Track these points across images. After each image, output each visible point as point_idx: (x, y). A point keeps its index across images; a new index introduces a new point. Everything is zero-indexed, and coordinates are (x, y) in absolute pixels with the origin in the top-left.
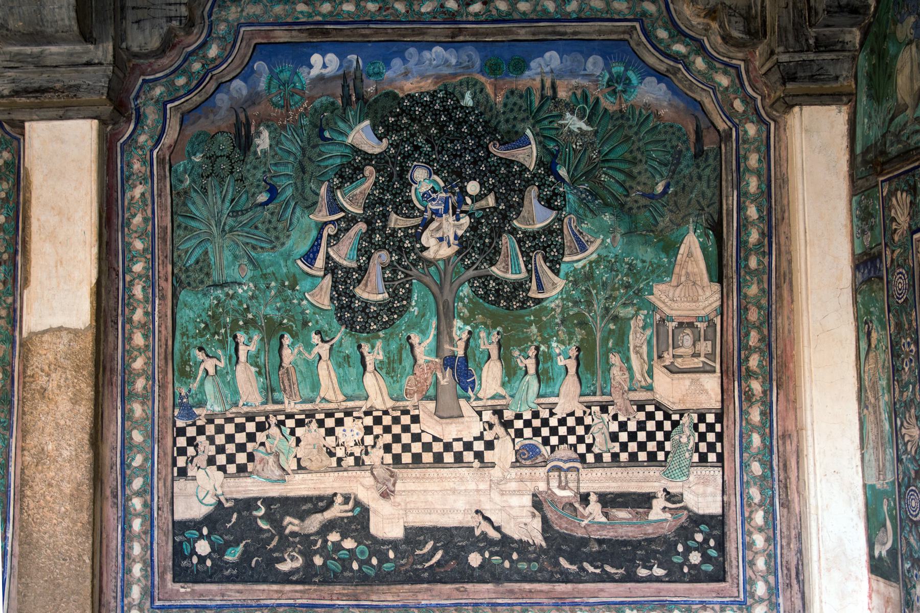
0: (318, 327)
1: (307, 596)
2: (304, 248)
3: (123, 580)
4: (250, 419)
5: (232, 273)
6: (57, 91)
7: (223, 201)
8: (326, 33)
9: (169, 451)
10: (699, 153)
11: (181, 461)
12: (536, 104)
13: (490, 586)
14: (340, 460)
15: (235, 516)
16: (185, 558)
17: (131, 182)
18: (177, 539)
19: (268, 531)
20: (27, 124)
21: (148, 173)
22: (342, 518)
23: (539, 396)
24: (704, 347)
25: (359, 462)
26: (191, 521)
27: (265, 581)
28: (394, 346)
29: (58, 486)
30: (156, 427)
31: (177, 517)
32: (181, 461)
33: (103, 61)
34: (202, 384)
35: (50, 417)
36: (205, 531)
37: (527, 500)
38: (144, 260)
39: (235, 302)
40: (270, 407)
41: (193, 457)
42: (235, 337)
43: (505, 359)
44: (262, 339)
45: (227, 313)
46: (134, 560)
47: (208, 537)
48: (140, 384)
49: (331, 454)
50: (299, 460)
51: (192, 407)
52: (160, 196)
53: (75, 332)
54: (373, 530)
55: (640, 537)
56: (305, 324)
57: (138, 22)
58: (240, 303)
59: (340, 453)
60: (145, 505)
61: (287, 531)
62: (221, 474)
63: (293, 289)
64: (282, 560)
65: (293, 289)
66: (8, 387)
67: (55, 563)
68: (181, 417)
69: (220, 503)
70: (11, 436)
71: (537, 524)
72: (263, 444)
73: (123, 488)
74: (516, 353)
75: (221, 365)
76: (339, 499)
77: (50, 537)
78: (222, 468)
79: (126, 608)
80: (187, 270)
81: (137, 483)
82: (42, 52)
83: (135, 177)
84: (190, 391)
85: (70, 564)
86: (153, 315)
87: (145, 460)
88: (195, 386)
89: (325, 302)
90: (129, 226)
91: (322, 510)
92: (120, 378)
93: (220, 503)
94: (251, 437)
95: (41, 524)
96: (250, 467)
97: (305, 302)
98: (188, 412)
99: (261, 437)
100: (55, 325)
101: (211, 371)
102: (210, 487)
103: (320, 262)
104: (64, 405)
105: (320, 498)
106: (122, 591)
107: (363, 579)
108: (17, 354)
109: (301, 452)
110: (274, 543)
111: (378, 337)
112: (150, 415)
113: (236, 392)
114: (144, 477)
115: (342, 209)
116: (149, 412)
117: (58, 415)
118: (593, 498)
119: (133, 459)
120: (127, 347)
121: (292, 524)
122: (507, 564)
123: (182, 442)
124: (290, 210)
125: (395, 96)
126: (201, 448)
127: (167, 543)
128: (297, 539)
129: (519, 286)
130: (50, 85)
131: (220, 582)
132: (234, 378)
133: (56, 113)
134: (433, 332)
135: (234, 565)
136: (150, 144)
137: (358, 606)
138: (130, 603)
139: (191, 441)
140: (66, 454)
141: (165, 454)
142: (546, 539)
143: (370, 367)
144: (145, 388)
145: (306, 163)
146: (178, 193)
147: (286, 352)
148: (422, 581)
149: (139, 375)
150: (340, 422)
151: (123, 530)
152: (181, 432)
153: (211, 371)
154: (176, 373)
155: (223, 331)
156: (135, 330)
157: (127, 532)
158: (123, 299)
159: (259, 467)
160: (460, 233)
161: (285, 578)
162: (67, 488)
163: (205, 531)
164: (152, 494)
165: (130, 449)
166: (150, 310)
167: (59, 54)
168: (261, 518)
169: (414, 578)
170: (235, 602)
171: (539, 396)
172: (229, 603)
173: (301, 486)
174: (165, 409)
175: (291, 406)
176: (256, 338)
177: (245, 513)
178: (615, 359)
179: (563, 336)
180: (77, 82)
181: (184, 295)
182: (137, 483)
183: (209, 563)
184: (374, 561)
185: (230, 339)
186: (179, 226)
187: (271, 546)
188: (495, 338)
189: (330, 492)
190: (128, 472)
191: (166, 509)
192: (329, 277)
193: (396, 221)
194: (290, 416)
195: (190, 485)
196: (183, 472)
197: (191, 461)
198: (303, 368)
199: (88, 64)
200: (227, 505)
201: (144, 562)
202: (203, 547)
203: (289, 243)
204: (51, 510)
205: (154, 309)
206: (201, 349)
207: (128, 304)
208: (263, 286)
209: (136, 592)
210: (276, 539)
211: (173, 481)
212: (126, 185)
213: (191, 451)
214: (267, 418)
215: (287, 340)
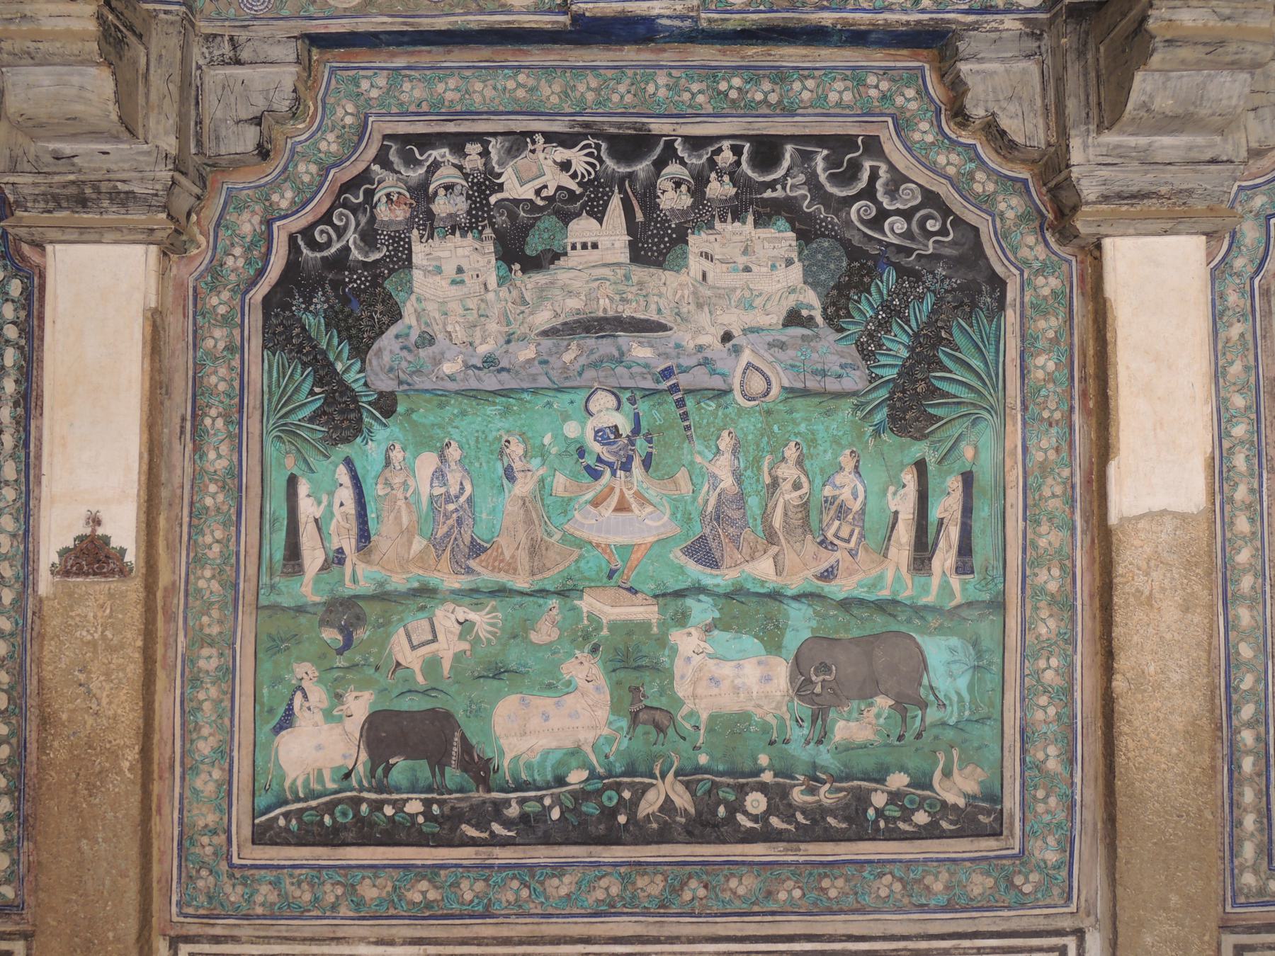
3: (1231, 835)
6: (1162, 197)
17: (1225, 319)
20: (1107, 243)
21: (1249, 308)
29: (1165, 719)
30: (1269, 639)
33: (1233, 159)
35: (1150, 630)
38: (1247, 420)
46: (1245, 810)
48: (1247, 583)
52: (1264, 337)
53: (1183, 518)
57: (1255, 109)
60: (1258, 739)
66: (1069, 588)
67: (1167, 820)
70: (1075, 652)
73: (1229, 717)
77: (1159, 787)
79: (1236, 871)
81: (1247, 711)
82: (1150, 145)
83: (1231, 313)
85: (1188, 821)
86: (1261, 492)
87: (1257, 681)
90: (1224, 376)
92: (1220, 575)
95: (1146, 770)
100: (1157, 507)
104: (1170, 612)
106: (1231, 850)
108: (1079, 544)
112: (1261, 624)
114: (1256, 702)
116: (1260, 619)
117: (1163, 627)
119: (1242, 680)
120: (1228, 535)
130: (1153, 189)
133: (1162, 226)
136: (1250, 269)
138: (1241, 864)
140: (1175, 677)
144: (1253, 588)
149: (1245, 572)
151: (1231, 772)
156: (1237, 513)
157: (1236, 774)
158: (1221, 472)
162: (1178, 722)
164: (1267, 725)
165: (1238, 667)
166: (1256, 486)
167: (1173, 147)
180: (1190, 186)
182: (1247, 711)
190: (1235, 697)
199: (1214, 161)
201: (1259, 812)
204: (1158, 751)
205: (1261, 486)
207: (1228, 478)
209: (1249, 850)
212: (1219, 323)
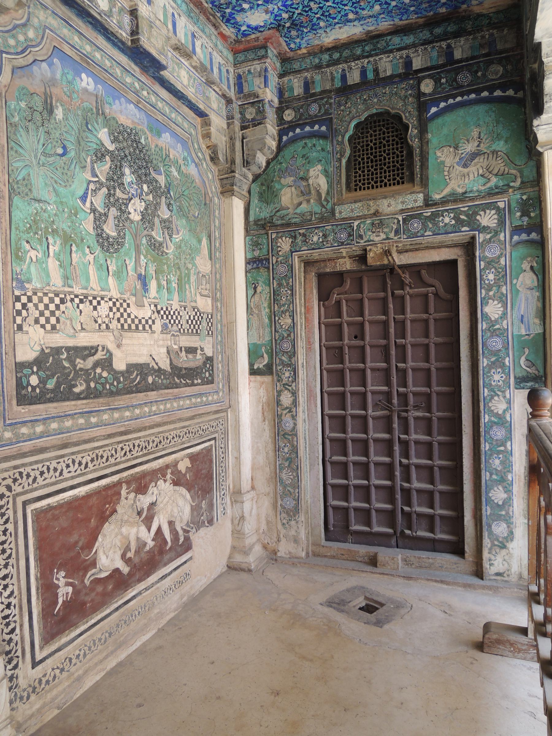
0: (88, 244)
1: (88, 406)
2: (81, 193)
4: (57, 295)
5: (44, 194)
7: (38, 142)
8: (88, 63)
9: (11, 312)
10: (205, 204)
11: (19, 320)
12: (164, 157)
13: (155, 392)
14: (100, 325)
15: (51, 358)
16: (24, 388)
18: (19, 375)
19: (69, 368)
22: (102, 359)
23: (168, 300)
24: (208, 286)
25: (108, 327)
26: (26, 362)
27: (68, 399)
28: (120, 264)
31: (18, 360)
32: (19, 320)
34: (29, 267)
36: (35, 369)
37: (165, 350)
39: (46, 215)
40: (67, 289)
41: (26, 318)
42: (47, 239)
43: (157, 279)
44: (61, 244)
45: (42, 220)
47: (37, 373)
49: (96, 322)
50: (82, 323)
51: (23, 282)
54: (114, 366)
55: (195, 366)
56: (82, 240)
58: (49, 217)
59: (100, 321)
61: (78, 368)
62: (43, 330)
63: (76, 217)
64: (75, 386)
65: (76, 217)
68: (18, 288)
69: (43, 350)
71: (168, 362)
72: (63, 312)
74: (161, 277)
75: (40, 256)
76: (100, 348)
78: (43, 326)
80: (17, 183)
84: (22, 270)
88: (25, 267)
89: (91, 230)
91: (94, 355)
93: (43, 350)
94: (58, 307)
96: (58, 326)
97: (81, 226)
98: (21, 284)
99: (62, 307)
101: (34, 259)
102: (37, 339)
103: (88, 204)
105: (92, 348)
107: (112, 394)
109: (82, 319)
110: (72, 375)
111: (113, 257)
113: (48, 276)
115: (97, 177)
118: (183, 349)
121: (80, 363)
122: (160, 381)
123: (18, 306)
124: (73, 166)
125: (117, 122)
126: (30, 311)
127: (12, 379)
128: (82, 373)
129: (161, 244)
131: (45, 402)
132: (47, 266)
134: (134, 260)
135: (52, 391)
137: (110, 409)
139: (24, 306)
141: (9, 314)
142: (171, 368)
143: (111, 273)
145: (80, 139)
146: (11, 124)
147: (74, 255)
148: (132, 392)
150: (99, 303)
152: (18, 299)
153: (34, 259)
154: (13, 256)
155: (40, 232)
159: (62, 327)
160: (142, 210)
161: (78, 397)
163: (35, 369)
168: (65, 359)
169: (129, 391)
170: (53, 415)
171: (168, 300)
172: (50, 416)
173: (84, 340)
174: (7, 281)
175: (77, 290)
176: (58, 242)
177: (56, 357)
178: (187, 287)
179: (174, 273)
181: (16, 200)
183: (38, 391)
184: (115, 383)
185: (44, 239)
186: (12, 148)
187: (71, 377)
188: (154, 268)
189: (96, 344)
191: (11, 354)
192: (92, 214)
193: (119, 193)
194: (77, 296)
195: (25, 337)
196: (20, 328)
197: (25, 320)
198: (82, 267)
200: (47, 351)
202: (34, 380)
203: (73, 186)
206: (28, 242)
208: (61, 210)
210: (73, 372)
211: (14, 333)
213: (24, 313)
214: (65, 295)
215: (74, 248)
